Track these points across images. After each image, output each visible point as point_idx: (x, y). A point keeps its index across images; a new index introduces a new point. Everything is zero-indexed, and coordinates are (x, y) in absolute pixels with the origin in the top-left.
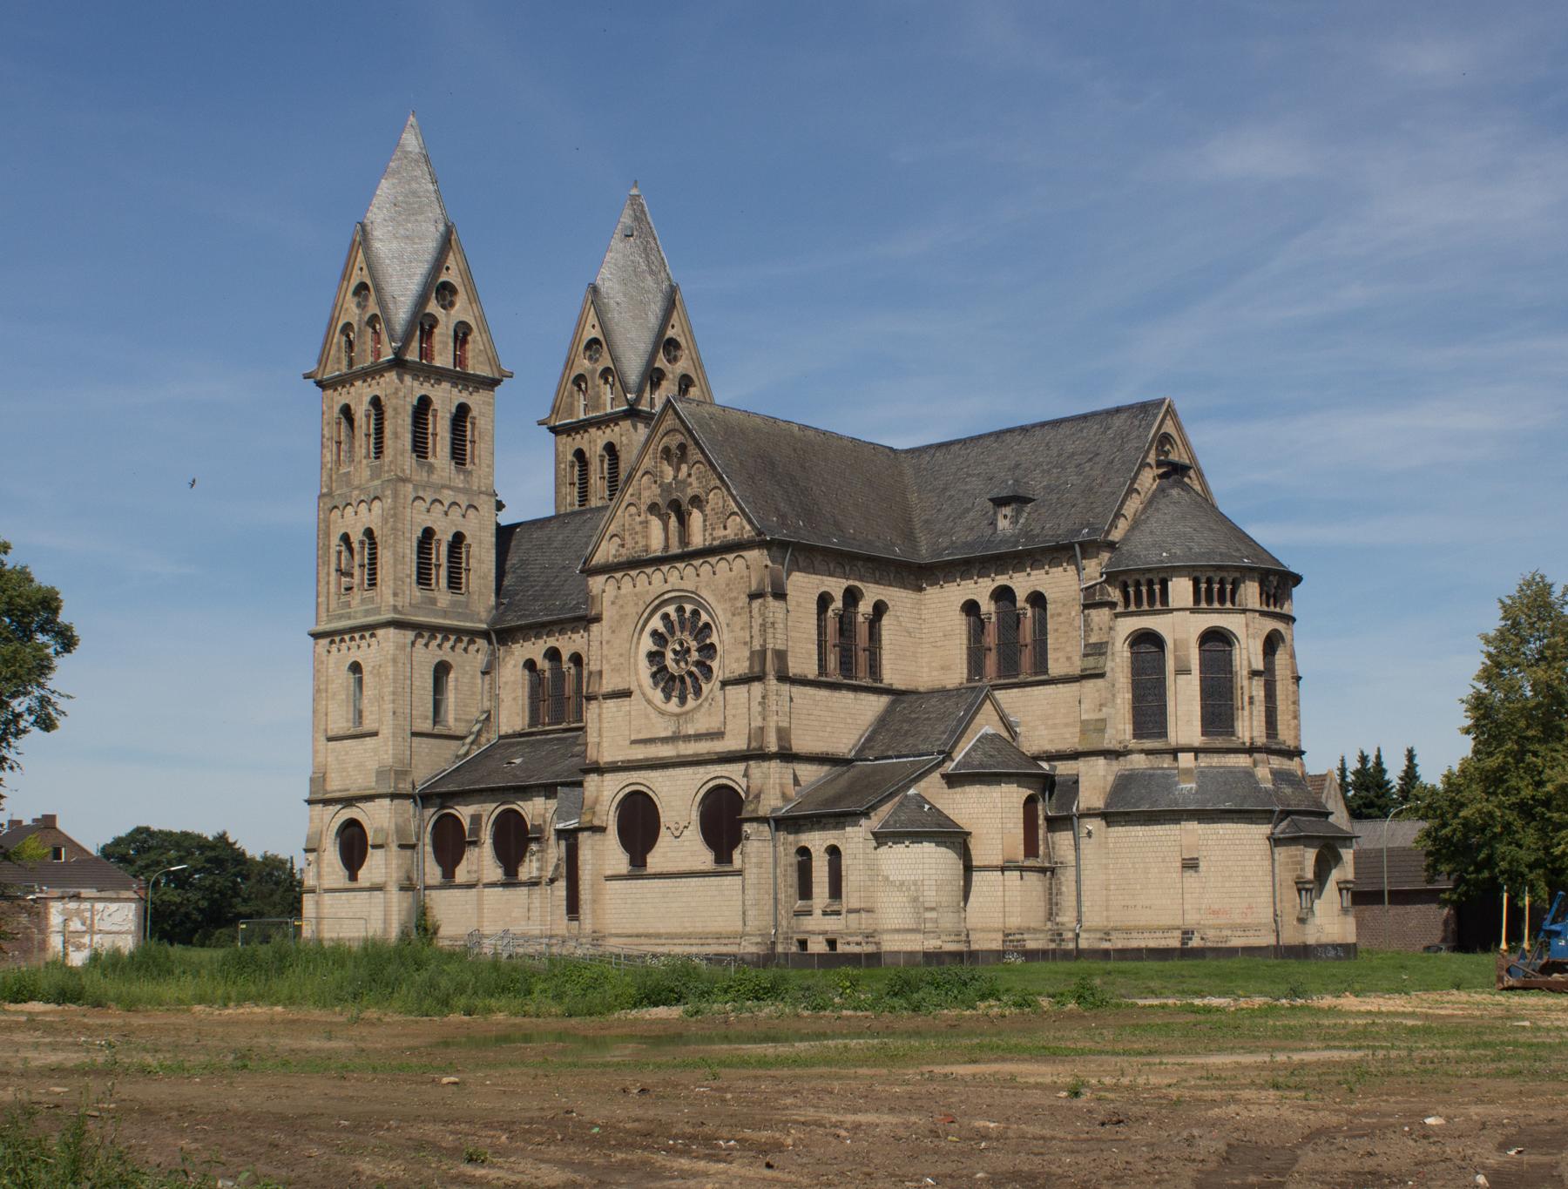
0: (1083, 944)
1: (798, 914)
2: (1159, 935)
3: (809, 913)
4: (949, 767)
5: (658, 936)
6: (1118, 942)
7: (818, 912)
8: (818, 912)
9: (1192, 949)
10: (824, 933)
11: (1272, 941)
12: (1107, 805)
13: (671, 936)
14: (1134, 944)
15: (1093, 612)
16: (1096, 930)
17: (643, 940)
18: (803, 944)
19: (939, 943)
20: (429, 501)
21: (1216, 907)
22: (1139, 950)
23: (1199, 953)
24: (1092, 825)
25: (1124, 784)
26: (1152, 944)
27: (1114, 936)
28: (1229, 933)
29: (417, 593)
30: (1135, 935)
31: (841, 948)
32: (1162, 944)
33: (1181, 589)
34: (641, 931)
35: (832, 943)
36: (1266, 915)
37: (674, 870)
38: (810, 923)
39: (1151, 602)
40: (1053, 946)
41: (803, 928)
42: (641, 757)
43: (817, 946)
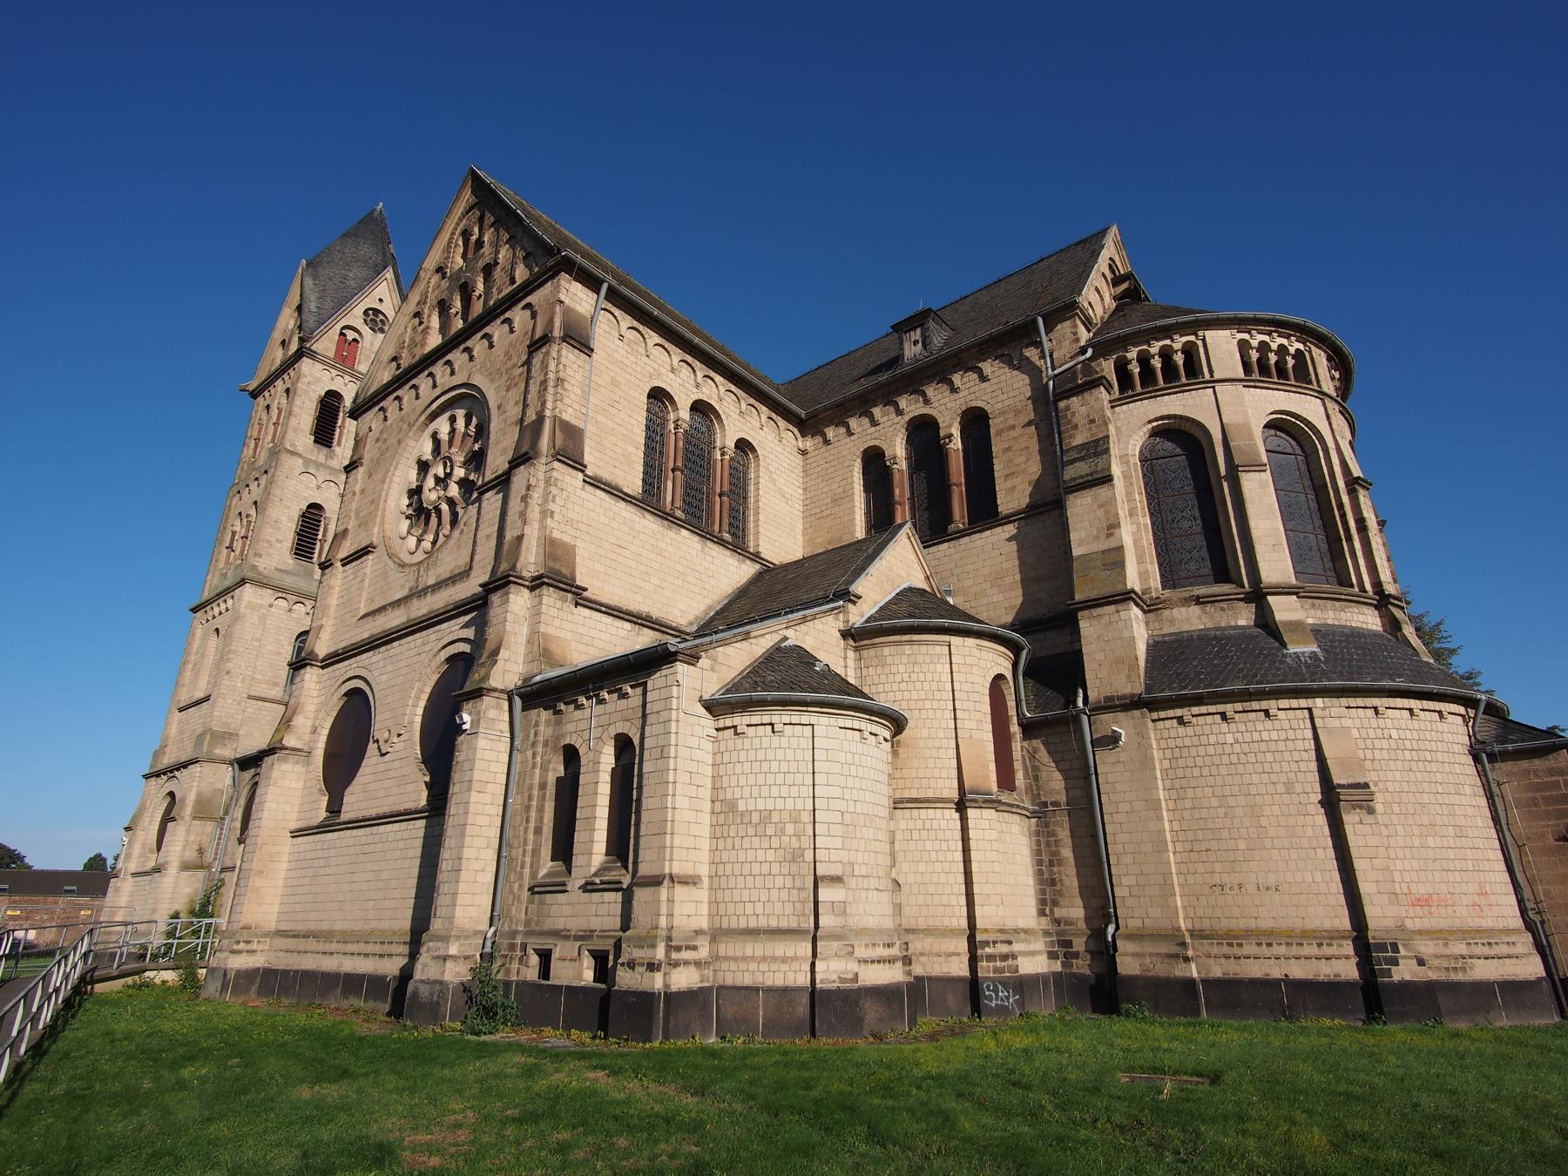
2: (1311, 950)
4: (858, 615)
5: (327, 936)
9: (1404, 985)
10: (585, 936)
11: (1532, 968)
12: (1148, 688)
13: (346, 937)
14: (1255, 970)
17: (311, 944)
19: (853, 966)
20: (321, 479)
21: (1421, 890)
23: (1427, 1000)
25: (1165, 652)
26: (1298, 971)
28: (1459, 948)
29: (290, 561)
34: (313, 926)
36: (1507, 912)
37: (373, 812)
40: (1057, 966)
41: (548, 924)
42: (366, 635)
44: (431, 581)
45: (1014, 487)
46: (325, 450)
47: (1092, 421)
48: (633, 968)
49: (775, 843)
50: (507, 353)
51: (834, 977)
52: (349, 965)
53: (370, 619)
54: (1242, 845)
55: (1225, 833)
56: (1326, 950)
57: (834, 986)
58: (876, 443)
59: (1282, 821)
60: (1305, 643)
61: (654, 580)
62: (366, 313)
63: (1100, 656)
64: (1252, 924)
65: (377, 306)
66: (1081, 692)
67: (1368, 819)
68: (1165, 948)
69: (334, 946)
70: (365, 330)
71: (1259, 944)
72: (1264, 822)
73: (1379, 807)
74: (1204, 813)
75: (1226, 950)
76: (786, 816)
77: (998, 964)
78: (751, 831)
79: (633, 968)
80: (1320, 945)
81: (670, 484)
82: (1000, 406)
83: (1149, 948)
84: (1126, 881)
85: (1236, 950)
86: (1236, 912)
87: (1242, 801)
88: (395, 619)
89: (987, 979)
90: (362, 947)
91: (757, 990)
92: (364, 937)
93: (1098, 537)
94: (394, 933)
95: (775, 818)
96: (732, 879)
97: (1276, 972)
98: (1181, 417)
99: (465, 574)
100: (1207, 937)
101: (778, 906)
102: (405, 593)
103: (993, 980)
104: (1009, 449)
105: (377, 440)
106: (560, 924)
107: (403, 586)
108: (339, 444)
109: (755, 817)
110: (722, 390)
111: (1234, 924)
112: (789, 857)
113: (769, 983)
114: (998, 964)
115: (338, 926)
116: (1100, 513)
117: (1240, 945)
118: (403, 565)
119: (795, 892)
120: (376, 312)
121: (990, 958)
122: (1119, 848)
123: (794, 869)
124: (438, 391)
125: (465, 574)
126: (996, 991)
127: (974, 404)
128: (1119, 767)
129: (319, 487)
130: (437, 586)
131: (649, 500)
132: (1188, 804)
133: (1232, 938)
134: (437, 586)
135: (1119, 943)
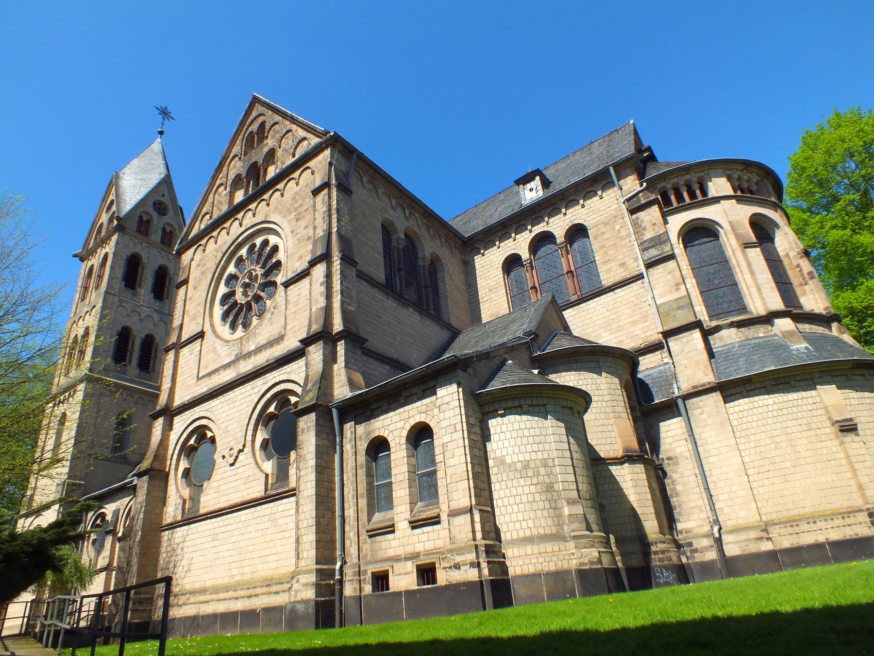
0: (731, 550)
1: (374, 534)
3: (390, 529)
6: (785, 540)
7: (402, 525)
8: (402, 525)
15: (641, 215)
16: (746, 529)
18: (381, 580)
22: (818, 547)
24: (843, 313)
27: (774, 532)
30: (804, 527)
31: (443, 577)
32: (849, 533)
33: (719, 186)
35: (427, 573)
38: (390, 546)
39: (692, 195)
41: (382, 554)
43: (403, 580)
44: (252, 347)
45: (610, 269)
46: (131, 291)
47: (654, 224)
48: (459, 568)
49: (535, 481)
50: (294, 199)
51: (586, 561)
52: (221, 608)
53: (207, 379)
54: (788, 464)
55: (777, 459)
56: (848, 521)
57: (587, 567)
58: (515, 252)
59: (809, 446)
60: (800, 343)
61: (398, 339)
62: (154, 204)
63: (685, 362)
64: (801, 511)
65: (161, 199)
66: (675, 386)
67: (856, 439)
68: (753, 534)
69: (207, 597)
70: (154, 214)
71: (809, 523)
72: (798, 448)
73: (860, 431)
74: (763, 449)
75: (790, 530)
76: (538, 462)
77: (660, 556)
78: (518, 475)
79: (459, 568)
80: (843, 518)
81: (397, 278)
82: (593, 221)
83: (743, 536)
84: (721, 498)
85: (796, 529)
86: (791, 506)
87: (784, 438)
88: (228, 376)
89: (657, 566)
90: (231, 594)
91: (540, 575)
92: (234, 588)
93: (671, 292)
94: (258, 581)
95: (532, 465)
96: (509, 508)
97: (821, 539)
98: (704, 219)
99: (280, 339)
100: (776, 524)
101: (543, 520)
102: (232, 358)
103: (660, 567)
104: (603, 246)
105: (198, 266)
106: (391, 553)
107: (229, 355)
108: (140, 287)
109: (519, 466)
110: (420, 222)
111: (791, 513)
112: (545, 489)
113: (546, 569)
114: (660, 556)
115: (209, 584)
116: (669, 277)
117: (797, 525)
118: (227, 341)
119: (552, 511)
120: (161, 203)
121: (656, 553)
122: (715, 478)
123: (549, 496)
124: (243, 229)
125: (280, 339)
126: (662, 573)
127: (576, 222)
128: (708, 428)
129: (128, 315)
130: (259, 350)
131: (388, 287)
132: (753, 444)
133: (791, 522)
134: (259, 350)
135: (723, 537)
